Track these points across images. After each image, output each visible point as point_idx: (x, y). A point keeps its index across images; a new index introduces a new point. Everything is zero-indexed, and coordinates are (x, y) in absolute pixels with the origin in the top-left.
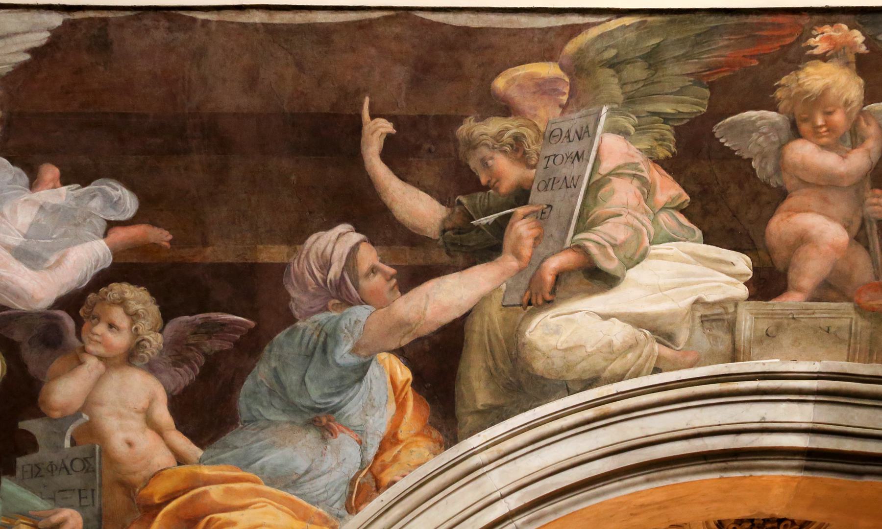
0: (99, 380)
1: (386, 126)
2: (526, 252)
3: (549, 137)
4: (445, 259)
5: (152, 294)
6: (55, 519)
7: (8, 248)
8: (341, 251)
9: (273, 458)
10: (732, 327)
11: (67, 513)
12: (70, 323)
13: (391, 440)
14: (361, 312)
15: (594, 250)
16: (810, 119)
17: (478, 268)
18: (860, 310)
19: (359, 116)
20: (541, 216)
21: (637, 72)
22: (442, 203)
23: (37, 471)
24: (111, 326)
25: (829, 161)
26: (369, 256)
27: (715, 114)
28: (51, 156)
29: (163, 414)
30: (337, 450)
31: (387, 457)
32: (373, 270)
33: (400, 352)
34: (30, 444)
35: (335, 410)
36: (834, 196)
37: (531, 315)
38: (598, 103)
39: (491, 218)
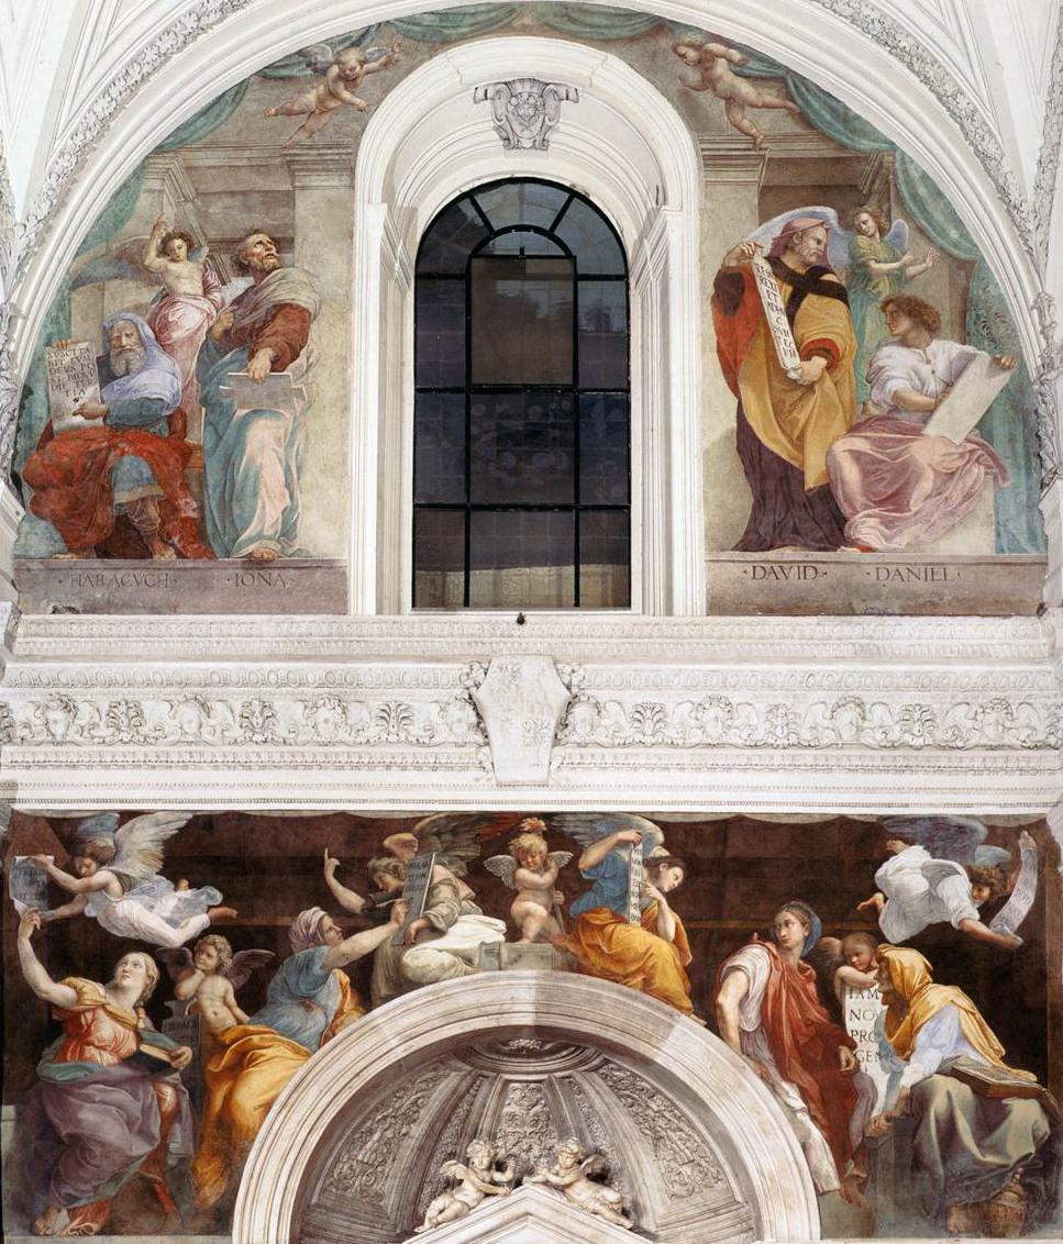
0: (201, 983)
1: (335, 862)
2: (402, 920)
3: (411, 866)
4: (363, 924)
5: (229, 940)
6: (179, 1052)
7: (163, 918)
8: (316, 919)
9: (283, 1021)
10: (499, 955)
11: (185, 1049)
12: (190, 954)
13: (340, 1012)
14: (325, 949)
15: (433, 918)
16: (526, 859)
17: (380, 928)
18: (558, 948)
19: (323, 858)
20: (408, 903)
21: (448, 837)
22: (362, 896)
23: (172, 1027)
24: (209, 955)
25: (535, 878)
26: (328, 922)
27: (483, 857)
28: (185, 875)
29: (231, 999)
30: (313, 1018)
31: (338, 1021)
32: (331, 929)
33: (345, 969)
34: (169, 1013)
35: (312, 998)
36: (539, 894)
37: (405, 950)
38: (431, 851)
39: (385, 904)
